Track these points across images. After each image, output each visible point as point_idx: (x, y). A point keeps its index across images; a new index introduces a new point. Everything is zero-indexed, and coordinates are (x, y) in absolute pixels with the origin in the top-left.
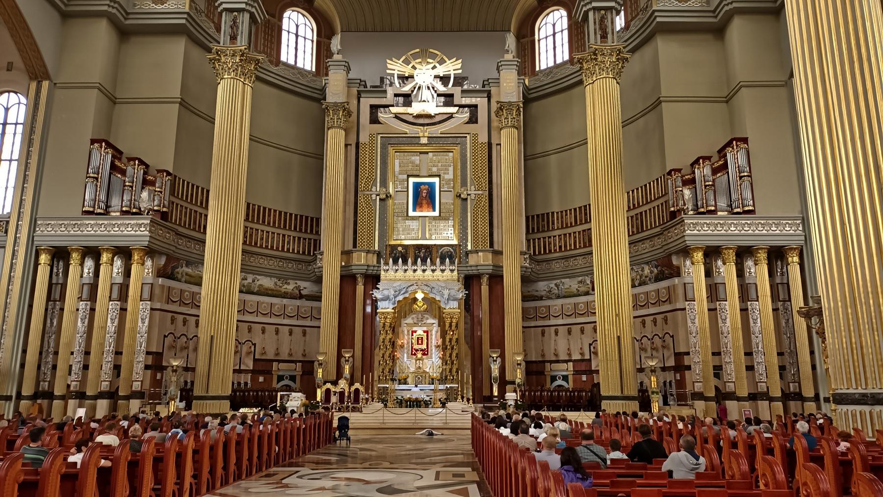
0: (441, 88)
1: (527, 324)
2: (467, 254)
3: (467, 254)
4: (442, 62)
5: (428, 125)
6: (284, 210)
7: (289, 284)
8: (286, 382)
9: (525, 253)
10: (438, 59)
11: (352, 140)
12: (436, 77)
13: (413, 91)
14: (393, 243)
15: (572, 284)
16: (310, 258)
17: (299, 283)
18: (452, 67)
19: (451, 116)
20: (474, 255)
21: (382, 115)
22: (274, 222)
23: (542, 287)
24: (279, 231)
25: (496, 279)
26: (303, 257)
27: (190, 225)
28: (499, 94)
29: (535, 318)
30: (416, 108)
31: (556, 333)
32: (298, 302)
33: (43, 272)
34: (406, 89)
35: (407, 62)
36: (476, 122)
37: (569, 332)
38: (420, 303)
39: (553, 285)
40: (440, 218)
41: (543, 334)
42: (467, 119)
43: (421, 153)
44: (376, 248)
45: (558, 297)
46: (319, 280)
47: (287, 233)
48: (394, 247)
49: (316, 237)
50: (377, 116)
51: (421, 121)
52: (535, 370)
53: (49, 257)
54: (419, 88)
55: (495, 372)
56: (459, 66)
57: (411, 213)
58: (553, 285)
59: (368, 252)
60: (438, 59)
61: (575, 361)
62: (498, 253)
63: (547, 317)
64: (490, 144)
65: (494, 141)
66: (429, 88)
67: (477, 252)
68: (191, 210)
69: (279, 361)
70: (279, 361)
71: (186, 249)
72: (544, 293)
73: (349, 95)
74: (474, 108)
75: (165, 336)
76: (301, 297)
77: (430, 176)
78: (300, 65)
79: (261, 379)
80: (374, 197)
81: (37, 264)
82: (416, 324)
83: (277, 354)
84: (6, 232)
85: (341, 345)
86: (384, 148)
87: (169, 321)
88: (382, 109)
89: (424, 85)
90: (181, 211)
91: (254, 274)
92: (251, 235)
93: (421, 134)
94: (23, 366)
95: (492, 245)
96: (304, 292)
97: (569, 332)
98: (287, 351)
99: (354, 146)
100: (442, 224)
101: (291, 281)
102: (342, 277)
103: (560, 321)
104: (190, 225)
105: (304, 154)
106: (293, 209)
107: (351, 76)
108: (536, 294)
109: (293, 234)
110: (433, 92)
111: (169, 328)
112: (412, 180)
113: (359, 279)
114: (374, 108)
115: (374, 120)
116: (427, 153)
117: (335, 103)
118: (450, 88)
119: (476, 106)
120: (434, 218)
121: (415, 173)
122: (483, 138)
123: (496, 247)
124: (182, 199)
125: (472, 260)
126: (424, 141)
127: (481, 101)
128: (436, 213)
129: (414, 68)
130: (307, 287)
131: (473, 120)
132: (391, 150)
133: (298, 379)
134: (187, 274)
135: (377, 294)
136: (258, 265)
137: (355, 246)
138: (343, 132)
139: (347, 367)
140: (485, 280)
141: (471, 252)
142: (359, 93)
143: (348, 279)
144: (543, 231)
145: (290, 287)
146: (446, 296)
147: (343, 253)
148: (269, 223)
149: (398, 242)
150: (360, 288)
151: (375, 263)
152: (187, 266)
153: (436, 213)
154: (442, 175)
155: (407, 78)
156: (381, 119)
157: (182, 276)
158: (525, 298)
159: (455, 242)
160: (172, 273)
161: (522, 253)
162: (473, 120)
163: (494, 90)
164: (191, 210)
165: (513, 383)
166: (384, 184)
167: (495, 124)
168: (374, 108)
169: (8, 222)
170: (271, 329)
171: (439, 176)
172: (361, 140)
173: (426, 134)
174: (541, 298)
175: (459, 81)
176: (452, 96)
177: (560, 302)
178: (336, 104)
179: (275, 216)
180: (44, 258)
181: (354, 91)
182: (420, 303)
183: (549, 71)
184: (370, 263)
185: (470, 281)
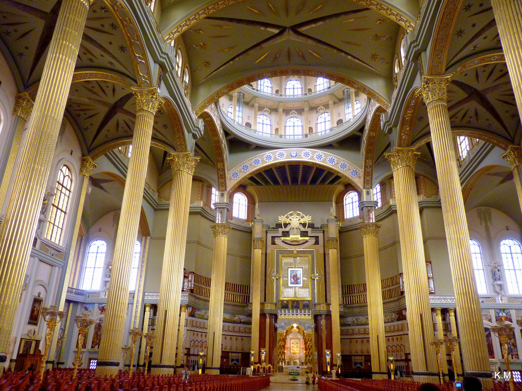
0: (303, 229)
1: (343, 337)
2: (315, 305)
3: (315, 305)
4: (303, 217)
5: (297, 245)
7: (235, 317)
8: (235, 362)
9: (341, 305)
10: (301, 216)
12: (300, 224)
14: (281, 299)
15: (362, 319)
16: (245, 305)
18: (307, 219)
19: (307, 241)
20: (319, 306)
21: (277, 241)
23: (350, 320)
24: (232, 293)
25: (328, 316)
26: (242, 304)
28: (328, 231)
29: (347, 334)
30: (292, 237)
31: (357, 342)
32: (239, 325)
34: (287, 229)
35: (287, 217)
36: (318, 244)
37: (362, 342)
39: (354, 319)
40: (303, 287)
41: (351, 342)
42: (314, 243)
45: (357, 325)
47: (235, 293)
48: (282, 301)
49: (248, 295)
51: (294, 243)
52: (346, 359)
55: (328, 358)
56: (310, 219)
57: (290, 285)
58: (354, 319)
60: (301, 216)
61: (365, 356)
62: (329, 305)
63: (353, 334)
64: (324, 254)
65: (326, 253)
67: (319, 304)
69: (232, 352)
70: (232, 352)
72: (350, 323)
74: (317, 238)
76: (241, 323)
79: (225, 360)
80: (273, 278)
82: (293, 338)
83: (231, 349)
85: (260, 347)
86: (278, 256)
95: (326, 301)
96: (242, 321)
97: (362, 342)
98: (235, 348)
100: (303, 290)
101: (237, 316)
103: (358, 336)
105: (242, 257)
106: (237, 282)
107: (264, 223)
108: (347, 323)
109: (237, 293)
115: (273, 243)
118: (306, 229)
119: (318, 237)
120: (300, 287)
122: (322, 252)
123: (328, 302)
125: (318, 308)
126: (295, 252)
127: (321, 235)
128: (301, 285)
129: (291, 220)
130: (243, 318)
131: (317, 243)
132: (280, 256)
133: (240, 360)
137: (265, 301)
140: (323, 316)
141: (317, 304)
144: (350, 293)
145: (236, 318)
146: (306, 327)
150: (268, 320)
151: (274, 309)
153: (301, 285)
155: (288, 224)
156: (276, 243)
158: (342, 325)
159: (310, 299)
161: (340, 305)
162: (317, 243)
163: (325, 229)
165: (336, 365)
167: (326, 244)
170: (228, 337)
172: (268, 252)
174: (350, 325)
175: (311, 226)
176: (307, 232)
177: (358, 327)
183: (351, 220)
185: (316, 318)
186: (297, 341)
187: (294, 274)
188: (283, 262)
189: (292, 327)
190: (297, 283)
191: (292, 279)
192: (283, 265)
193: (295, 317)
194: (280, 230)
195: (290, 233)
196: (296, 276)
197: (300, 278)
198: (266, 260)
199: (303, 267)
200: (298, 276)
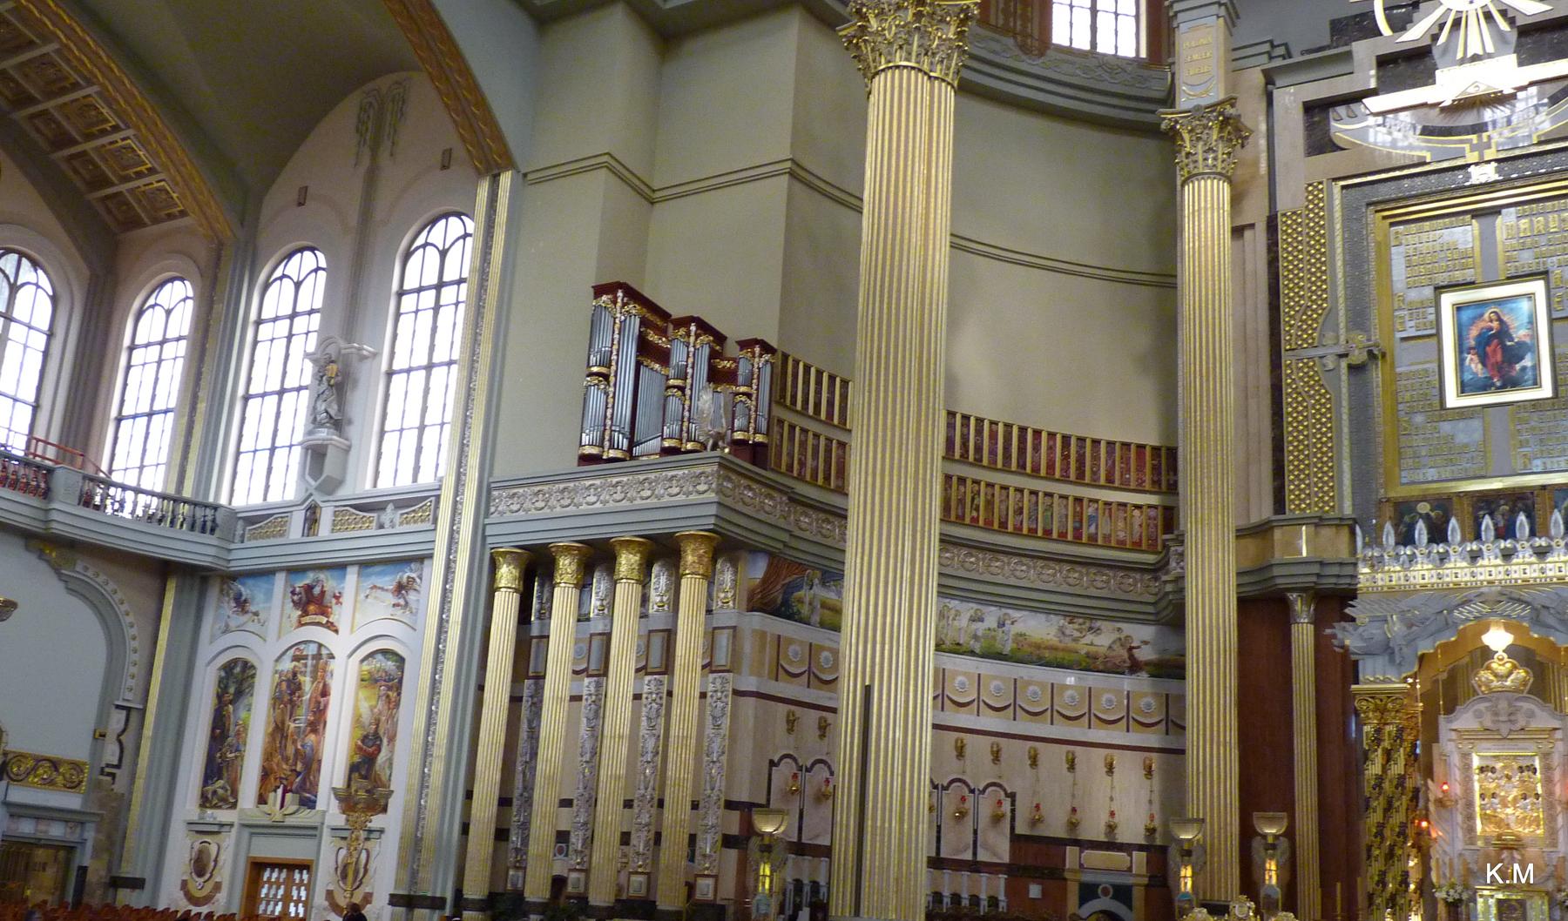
6: (1075, 432)
11: (1256, 212)
13: (1435, 37)
17: (1129, 629)
22: (1051, 466)
27: (827, 478)
30: (1449, 84)
33: (505, 606)
38: (1501, 664)
43: (1476, 214)
44: (1348, 510)
46: (1173, 618)
50: (1327, 131)
53: (516, 573)
54: (1457, 23)
59: (1319, 522)
66: (1488, 16)
68: (829, 440)
71: (818, 539)
73: (1232, 83)
75: (772, 764)
77: (1513, 279)
78: (1105, 47)
81: (492, 590)
84: (435, 521)
86: (1353, 217)
87: (781, 726)
88: (1342, 110)
89: (1472, 11)
90: (803, 444)
91: (1001, 605)
92: (990, 503)
93: (1472, 157)
94: (465, 829)
99: (1261, 227)
101: (1105, 625)
102: (1242, 601)
104: (827, 478)
110: (1504, 26)
111: (781, 743)
112: (1448, 300)
113: (1298, 606)
114: (1317, 110)
115: (1320, 142)
116: (1496, 211)
117: (1198, 108)
121: (1459, 276)
124: (803, 413)
128: (1546, 391)
134: (824, 606)
135: (1349, 638)
136: (1013, 581)
138: (1225, 188)
139: (1272, 866)
142: (1269, 78)
143: (1262, 607)
147: (1241, 533)
148: (1036, 469)
149: (1415, 491)
150: (1303, 633)
152: (824, 583)
153: (1546, 391)
154: (1556, 272)
157: (813, 609)
160: (786, 602)
164: (829, 440)
166: (1358, 319)
168: (1317, 110)
169: (438, 497)
171: (1544, 274)
173: (1490, 154)
178: (1197, 112)
179: (1051, 448)
180: (507, 574)
181: (1257, 78)
182: (1501, 664)
184: (1328, 556)
186: (1529, 752)
187: (1488, 320)
188: (1398, 257)
189: (1487, 653)
190: (1512, 383)
191: (1475, 366)
192: (1399, 271)
193: (1491, 569)
194: (1365, 51)
195: (1436, 52)
196: (1503, 332)
197: (1533, 348)
198: (1273, 262)
199: (1552, 263)
200: (1520, 334)
